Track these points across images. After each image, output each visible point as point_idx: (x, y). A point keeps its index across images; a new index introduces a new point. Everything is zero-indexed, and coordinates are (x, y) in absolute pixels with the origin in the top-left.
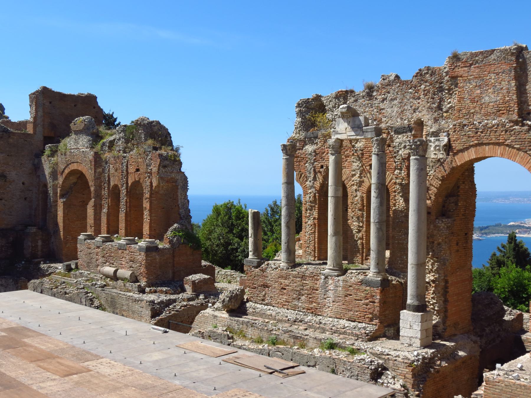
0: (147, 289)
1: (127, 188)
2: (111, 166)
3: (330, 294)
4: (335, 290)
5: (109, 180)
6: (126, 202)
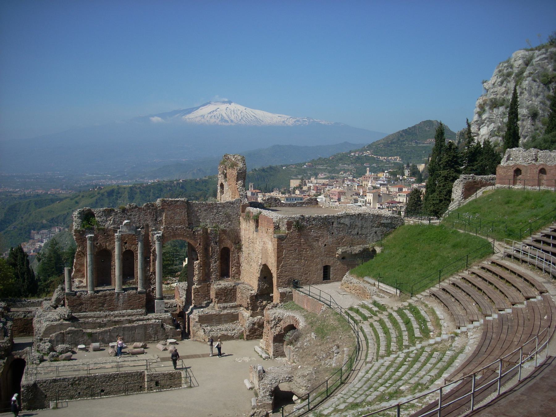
4: (123, 298)
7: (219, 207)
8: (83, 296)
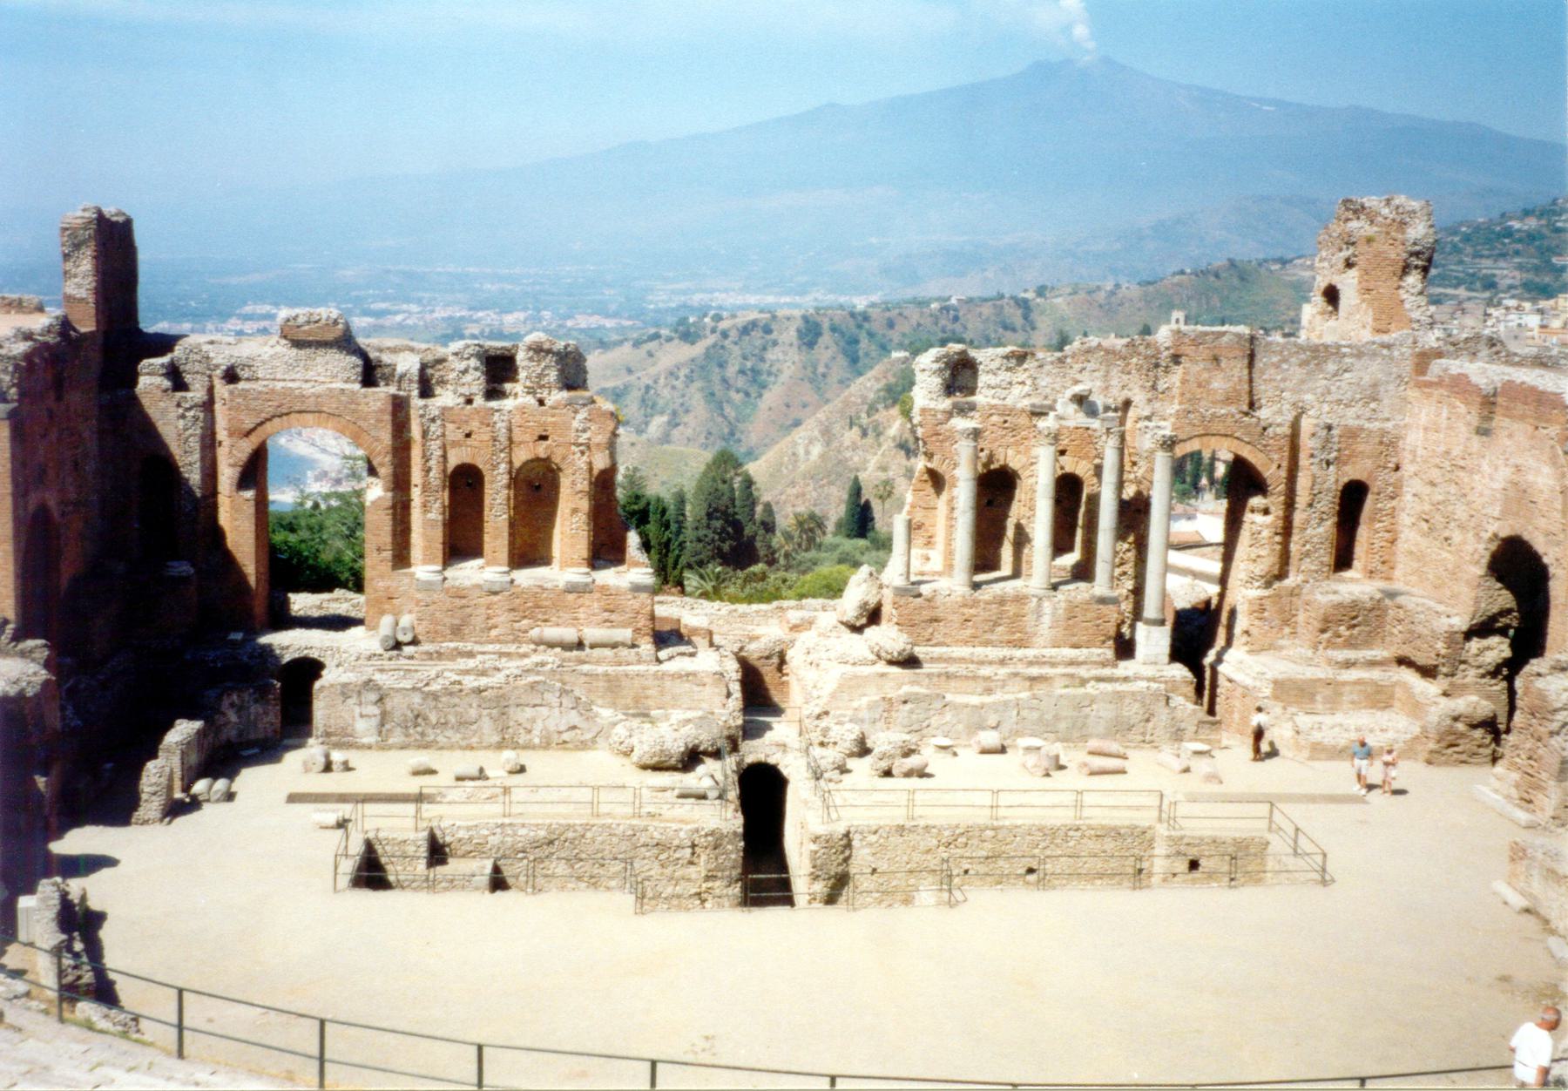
0: (663, 654)
1: (510, 473)
2: (450, 426)
3: (1047, 620)
4: (1053, 614)
5: (444, 457)
6: (509, 499)
7: (1345, 355)
8: (939, 600)
